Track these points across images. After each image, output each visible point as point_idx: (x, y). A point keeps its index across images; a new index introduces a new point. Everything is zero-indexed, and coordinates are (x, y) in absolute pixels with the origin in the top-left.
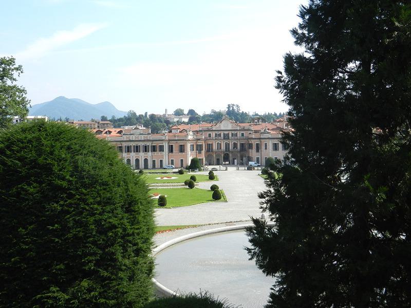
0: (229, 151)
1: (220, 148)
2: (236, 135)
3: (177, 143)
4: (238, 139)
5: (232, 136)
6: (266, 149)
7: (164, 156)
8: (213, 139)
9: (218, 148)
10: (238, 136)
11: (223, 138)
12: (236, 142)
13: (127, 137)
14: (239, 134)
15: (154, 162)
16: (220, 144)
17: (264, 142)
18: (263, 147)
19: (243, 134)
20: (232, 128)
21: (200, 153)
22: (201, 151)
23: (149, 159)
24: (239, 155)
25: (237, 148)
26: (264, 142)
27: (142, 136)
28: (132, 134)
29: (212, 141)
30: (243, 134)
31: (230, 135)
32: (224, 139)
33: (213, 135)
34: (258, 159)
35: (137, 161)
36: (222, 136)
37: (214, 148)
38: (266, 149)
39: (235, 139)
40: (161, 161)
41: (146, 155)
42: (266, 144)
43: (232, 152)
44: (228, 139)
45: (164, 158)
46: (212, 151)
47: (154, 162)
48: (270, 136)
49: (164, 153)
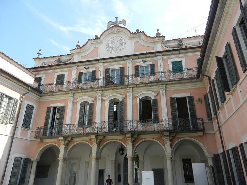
0: (122, 131)
1: (91, 122)
2: (153, 69)
4: (156, 83)
5: (137, 74)
8: (68, 91)
9: (81, 123)
11: (101, 83)
12: (152, 96)
16: (92, 106)
19: (178, 67)
20: (135, 50)
25: (157, 119)
29: (64, 97)
30: (178, 67)
31: (130, 72)
32: (108, 83)
33: (70, 75)
36: (101, 75)
37: (67, 120)
39: (145, 85)
43: (135, 136)
44: (122, 83)
46: (59, 133)
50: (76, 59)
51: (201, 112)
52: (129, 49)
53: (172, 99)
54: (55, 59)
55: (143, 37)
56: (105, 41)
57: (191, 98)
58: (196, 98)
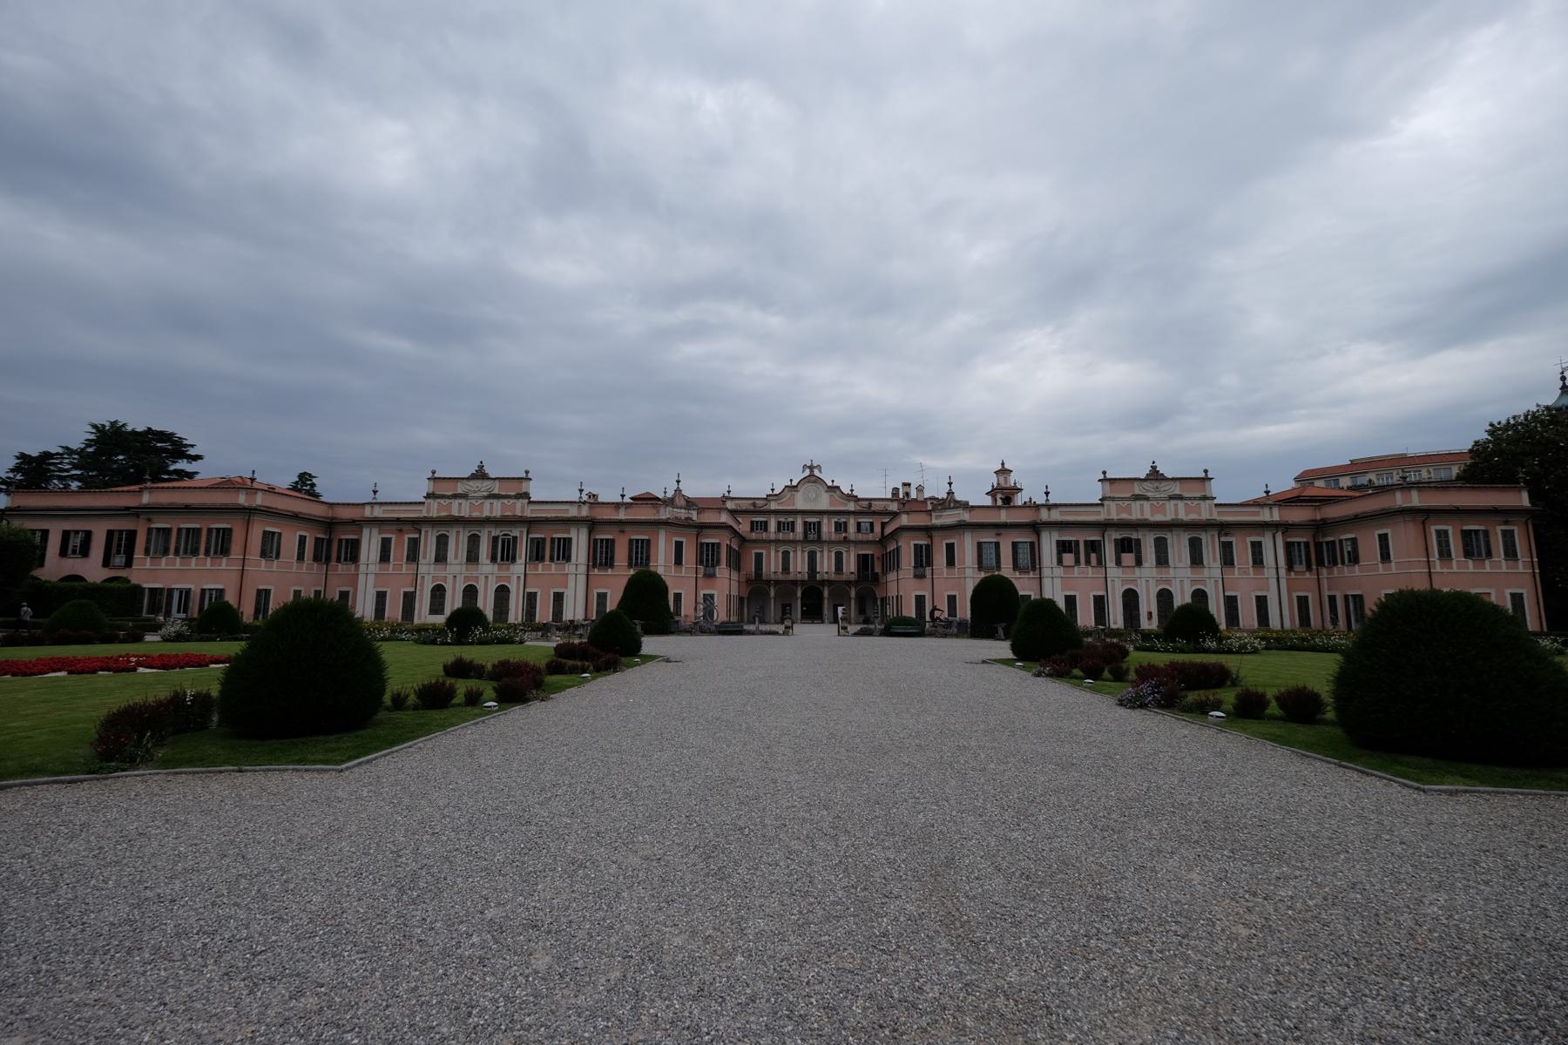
3: (623, 532)
6: (951, 562)
7: (571, 579)
11: (800, 536)
13: (440, 507)
15: (531, 599)
18: (940, 558)
21: (710, 576)
22: (713, 566)
23: (513, 587)
24: (853, 594)
27: (497, 504)
28: (464, 496)
36: (799, 528)
38: (951, 562)
40: (559, 598)
41: (504, 574)
42: (950, 548)
44: (819, 536)
45: (571, 584)
47: (531, 599)
48: (966, 516)
49: (569, 568)
50: (773, 506)
51: (878, 569)
52: (824, 503)
53: (859, 555)
54: (751, 502)
55: (838, 492)
56: (802, 489)
57: (872, 555)
58: (875, 557)
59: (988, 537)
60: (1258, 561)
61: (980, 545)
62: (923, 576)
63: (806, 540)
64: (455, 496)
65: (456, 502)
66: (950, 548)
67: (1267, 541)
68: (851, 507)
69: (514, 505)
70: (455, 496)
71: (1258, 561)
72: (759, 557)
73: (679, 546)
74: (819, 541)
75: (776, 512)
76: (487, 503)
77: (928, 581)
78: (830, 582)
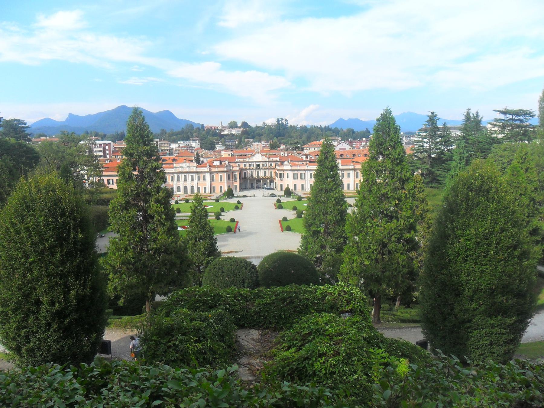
6: (288, 177)
10: (267, 166)
14: (268, 165)
15: (199, 189)
17: (286, 173)
18: (285, 176)
19: (271, 165)
20: (263, 159)
26: (286, 173)
30: (271, 165)
31: (261, 166)
34: (281, 185)
35: (186, 187)
36: (255, 166)
38: (288, 177)
40: (205, 188)
42: (288, 174)
45: (207, 184)
47: (199, 189)
59: (296, 172)
60: (349, 177)
61: (294, 174)
62: (282, 180)
63: (256, 168)
64: (180, 167)
65: (180, 168)
66: (288, 174)
67: (351, 172)
68: (267, 160)
69: (193, 169)
70: (180, 167)
71: (349, 177)
72: (245, 173)
73: (229, 175)
74: (260, 169)
75: (249, 162)
76: (187, 168)
77: (283, 181)
78: (263, 179)
